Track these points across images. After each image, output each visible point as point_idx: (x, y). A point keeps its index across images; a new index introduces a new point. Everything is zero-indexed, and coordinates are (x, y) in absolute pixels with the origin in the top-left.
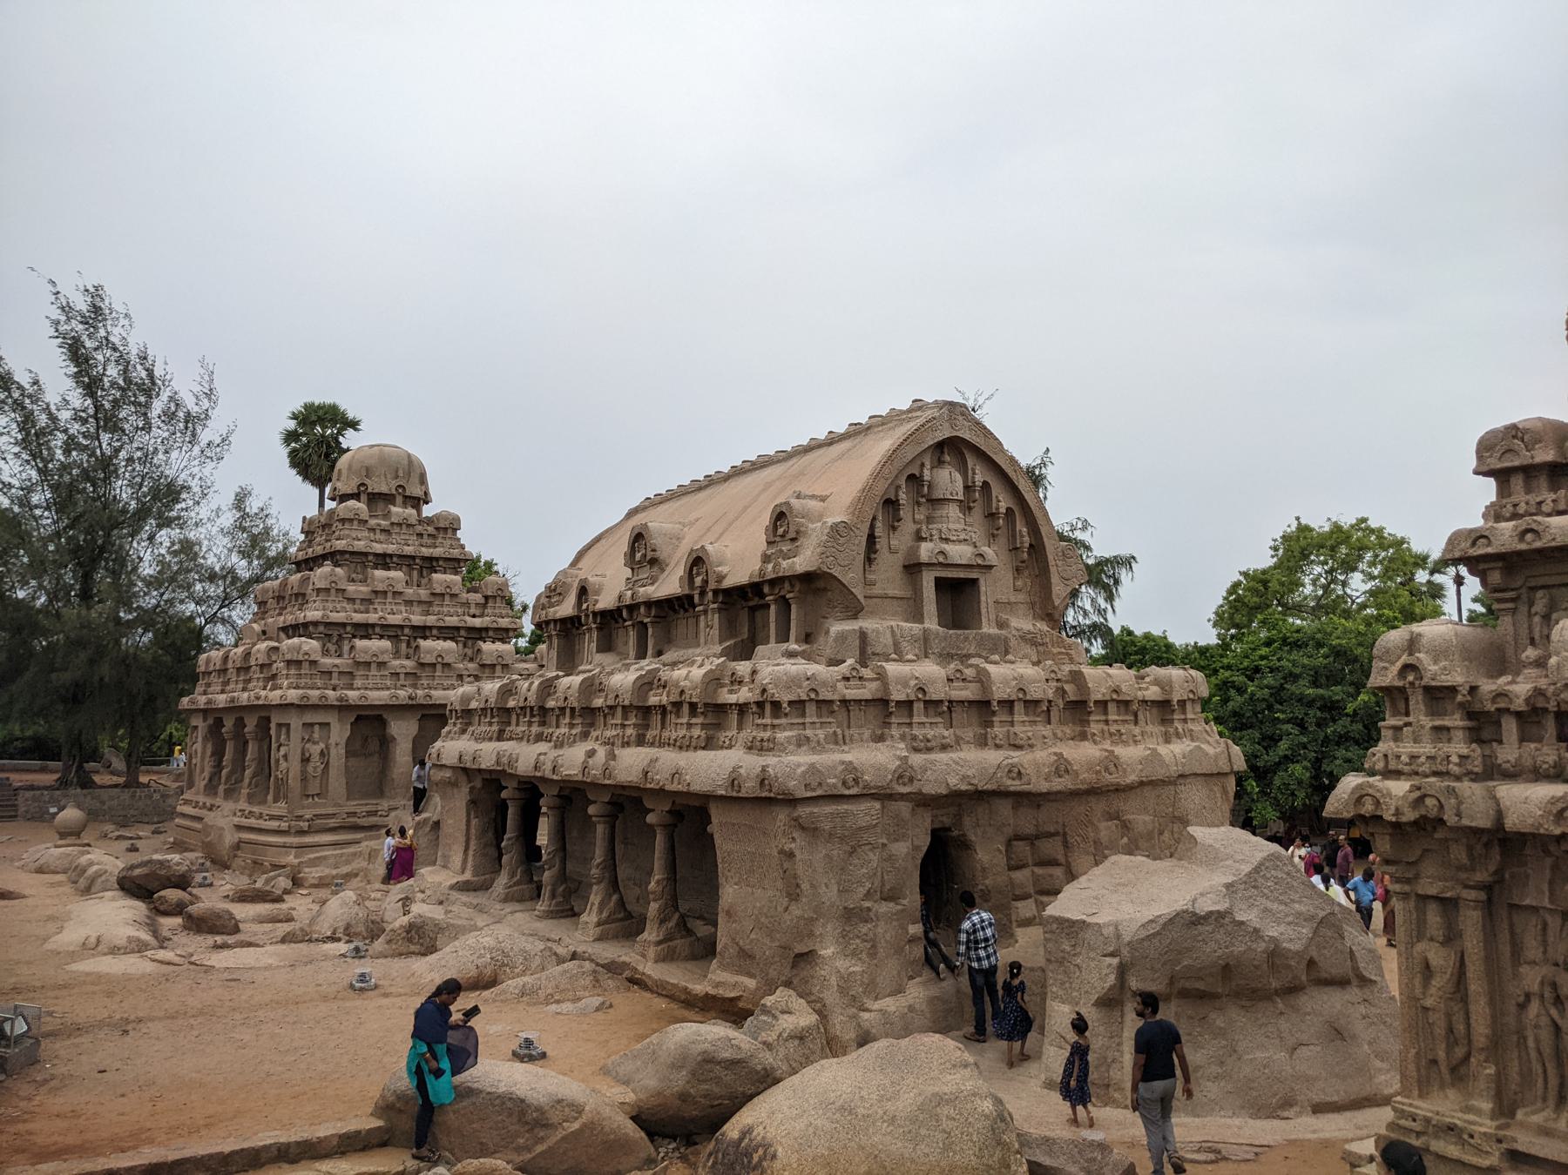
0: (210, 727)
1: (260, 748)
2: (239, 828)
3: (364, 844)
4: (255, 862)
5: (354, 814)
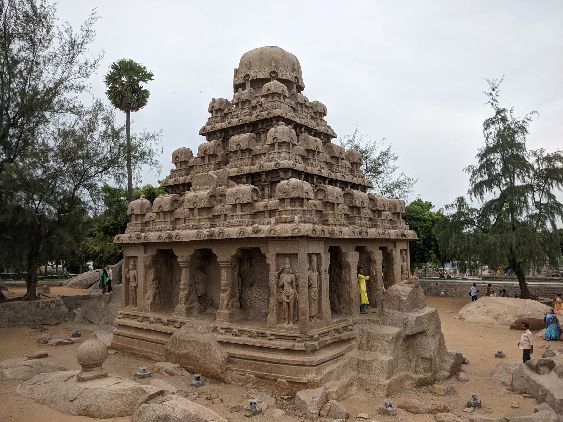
0: (153, 257)
1: (233, 274)
2: (223, 343)
3: (348, 355)
4: (261, 377)
5: (337, 330)
